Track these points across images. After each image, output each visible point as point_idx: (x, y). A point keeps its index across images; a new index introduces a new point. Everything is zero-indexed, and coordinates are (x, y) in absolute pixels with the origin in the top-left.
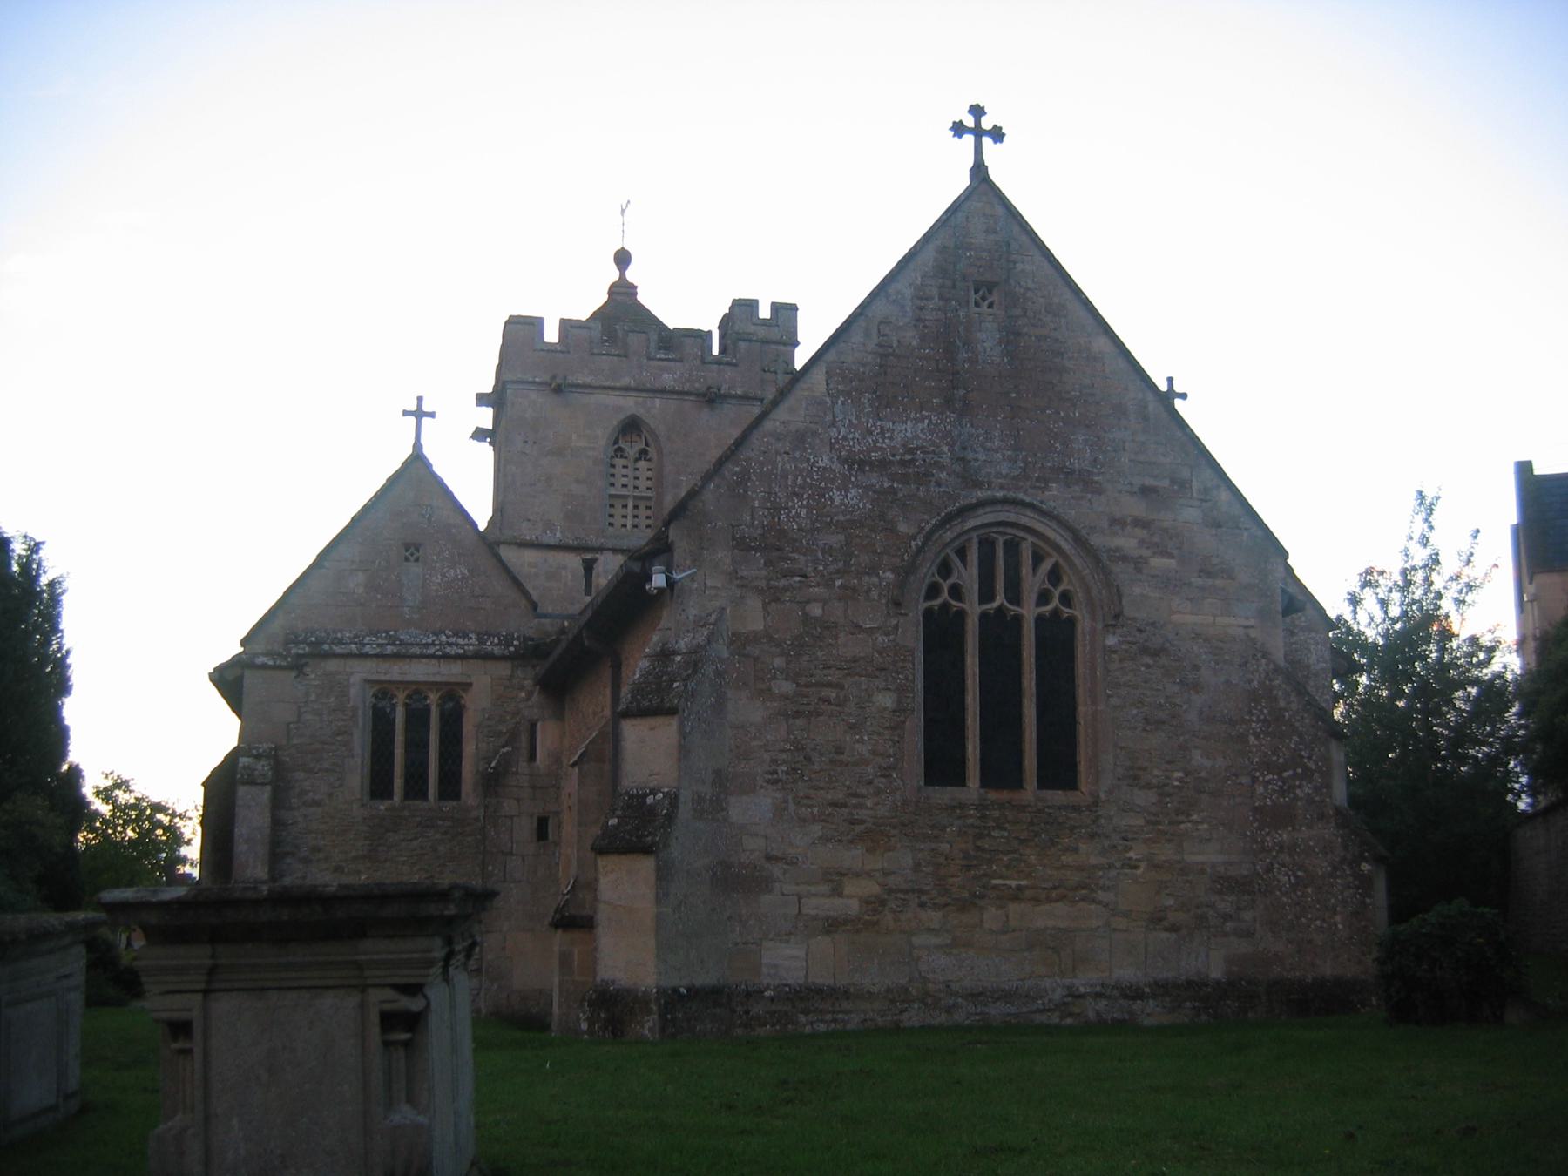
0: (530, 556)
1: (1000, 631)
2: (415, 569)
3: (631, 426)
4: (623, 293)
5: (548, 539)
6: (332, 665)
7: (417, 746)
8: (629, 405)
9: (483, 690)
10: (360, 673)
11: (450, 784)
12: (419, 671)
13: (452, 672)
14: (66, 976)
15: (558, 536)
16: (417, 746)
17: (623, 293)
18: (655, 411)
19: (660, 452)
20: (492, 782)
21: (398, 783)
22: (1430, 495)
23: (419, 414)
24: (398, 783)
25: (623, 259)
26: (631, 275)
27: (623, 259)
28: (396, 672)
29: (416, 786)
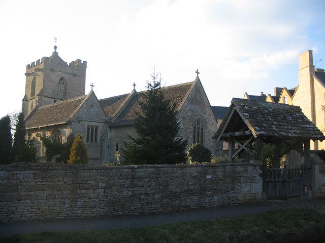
0: (47, 99)
1: (198, 128)
2: (92, 109)
3: (62, 79)
4: (55, 54)
5: (49, 96)
6: (83, 122)
7: (92, 132)
8: (63, 75)
9: (101, 127)
10: (86, 124)
11: (96, 141)
12: (93, 124)
13: (97, 124)
14: (293, 190)
15: (51, 96)
16: (92, 132)
17: (55, 54)
18: (66, 76)
19: (66, 83)
20: (102, 140)
21: (94, 141)
22: (136, 84)
23: (92, 86)
24: (94, 141)
25: (55, 48)
26: (57, 51)
27: (55, 48)
28: (91, 124)
29: (92, 141)
